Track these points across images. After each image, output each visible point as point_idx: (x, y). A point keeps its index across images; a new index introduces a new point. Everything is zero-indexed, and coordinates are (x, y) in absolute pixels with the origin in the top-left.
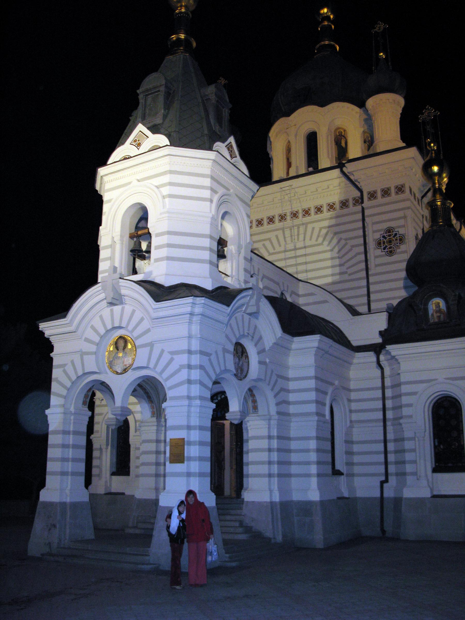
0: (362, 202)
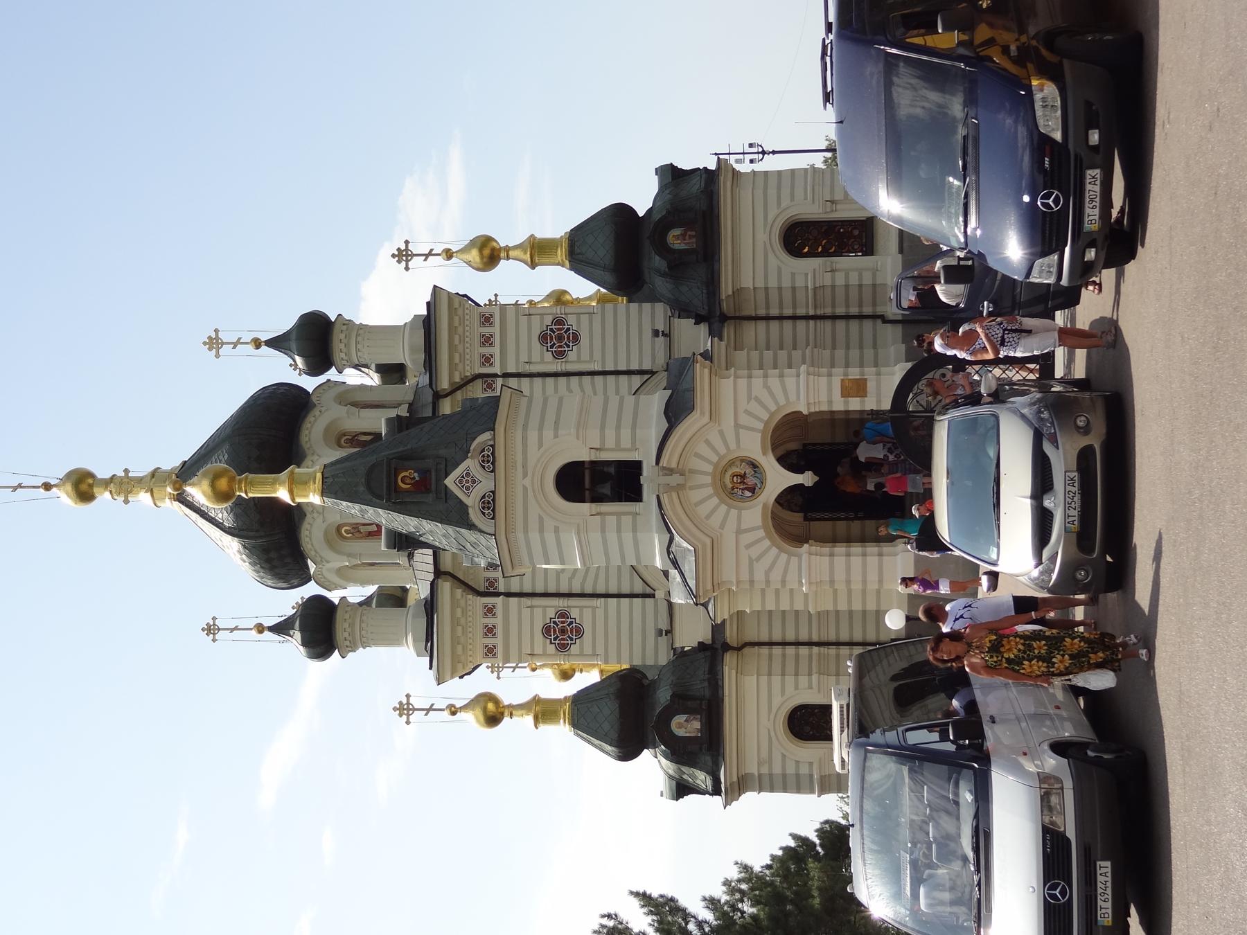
0: (495, 376)
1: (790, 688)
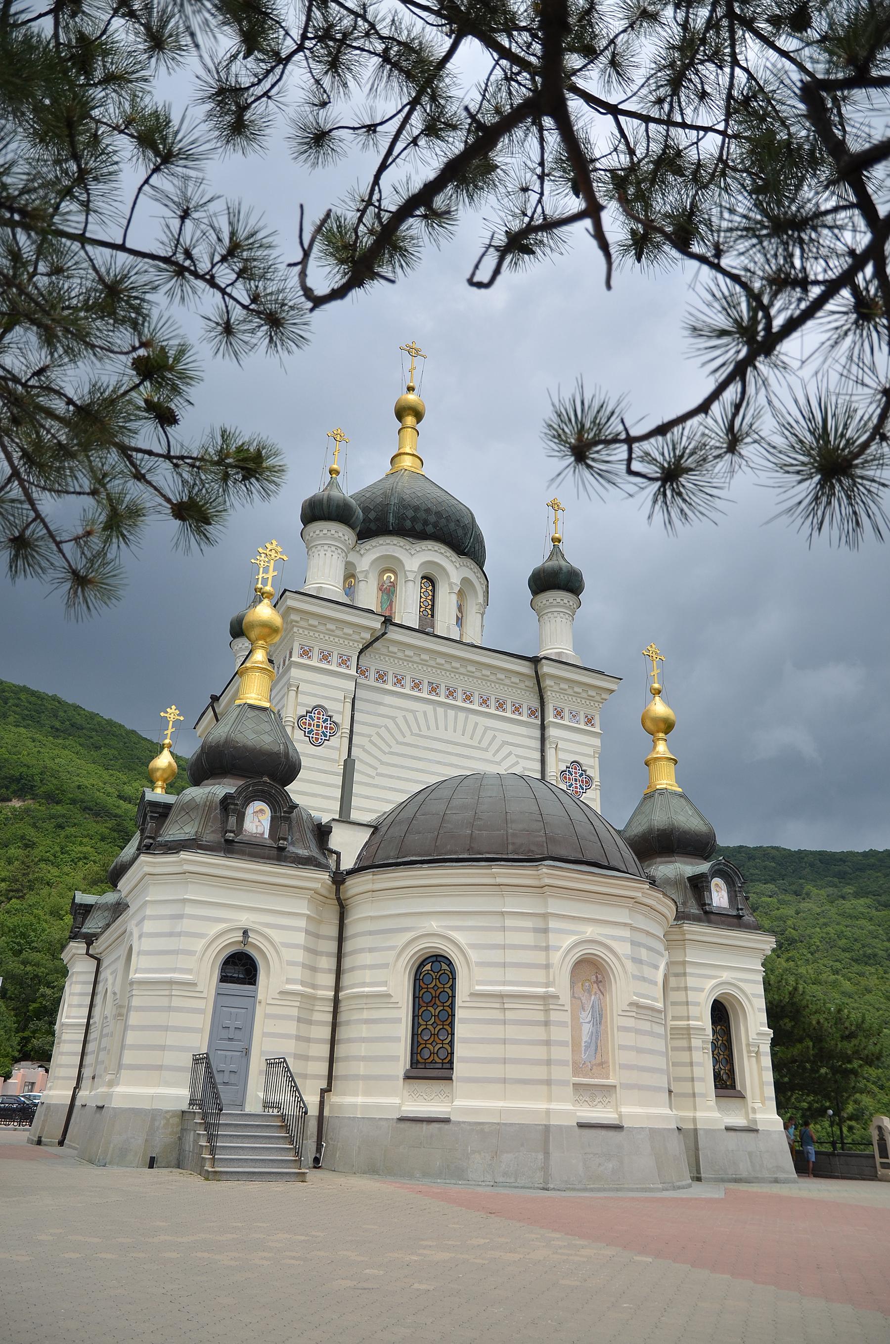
1: (288, 954)
